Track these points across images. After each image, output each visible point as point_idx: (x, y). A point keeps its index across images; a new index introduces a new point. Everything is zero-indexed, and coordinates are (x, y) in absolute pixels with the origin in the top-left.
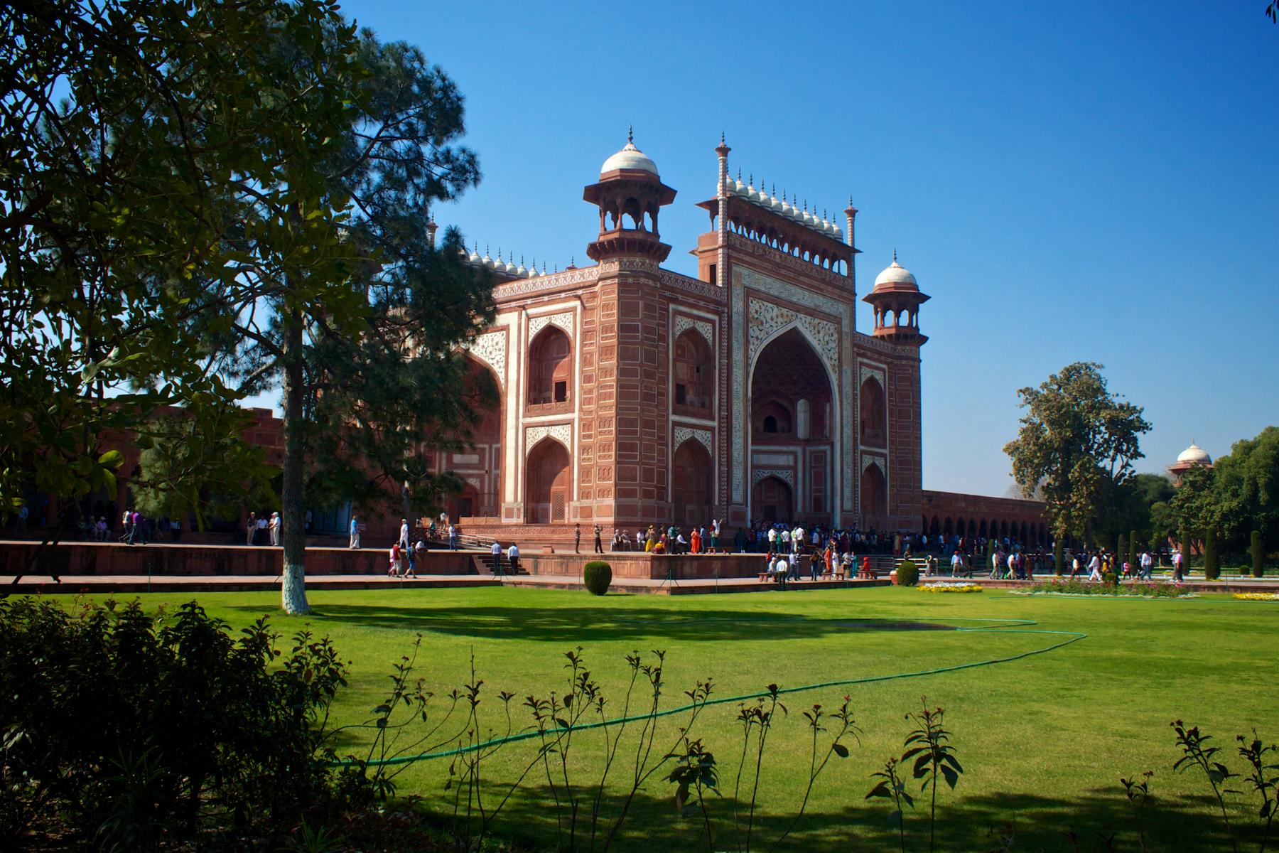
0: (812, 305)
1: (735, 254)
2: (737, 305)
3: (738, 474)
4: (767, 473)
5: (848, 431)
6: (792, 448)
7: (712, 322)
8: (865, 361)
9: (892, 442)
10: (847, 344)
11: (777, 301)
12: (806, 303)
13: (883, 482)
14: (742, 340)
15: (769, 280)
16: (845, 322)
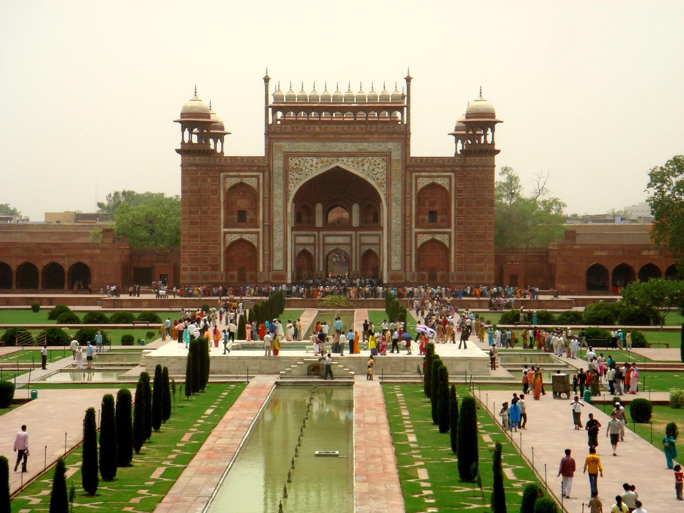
0: (356, 150)
1: (276, 136)
2: (278, 164)
3: (278, 255)
4: (366, 248)
5: (397, 221)
6: (378, 232)
7: (258, 177)
8: (423, 174)
9: (458, 224)
10: (397, 168)
11: (317, 155)
12: (349, 150)
13: (447, 251)
14: (282, 183)
15: (308, 144)
16: (396, 155)
